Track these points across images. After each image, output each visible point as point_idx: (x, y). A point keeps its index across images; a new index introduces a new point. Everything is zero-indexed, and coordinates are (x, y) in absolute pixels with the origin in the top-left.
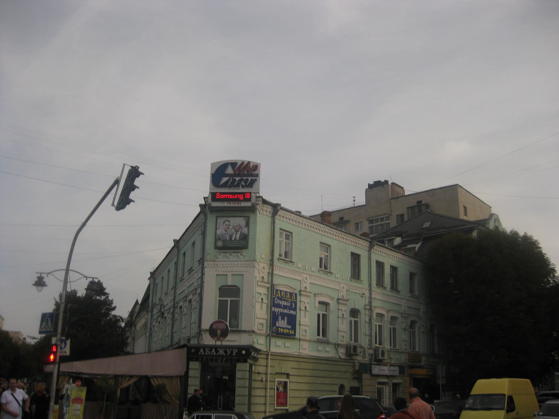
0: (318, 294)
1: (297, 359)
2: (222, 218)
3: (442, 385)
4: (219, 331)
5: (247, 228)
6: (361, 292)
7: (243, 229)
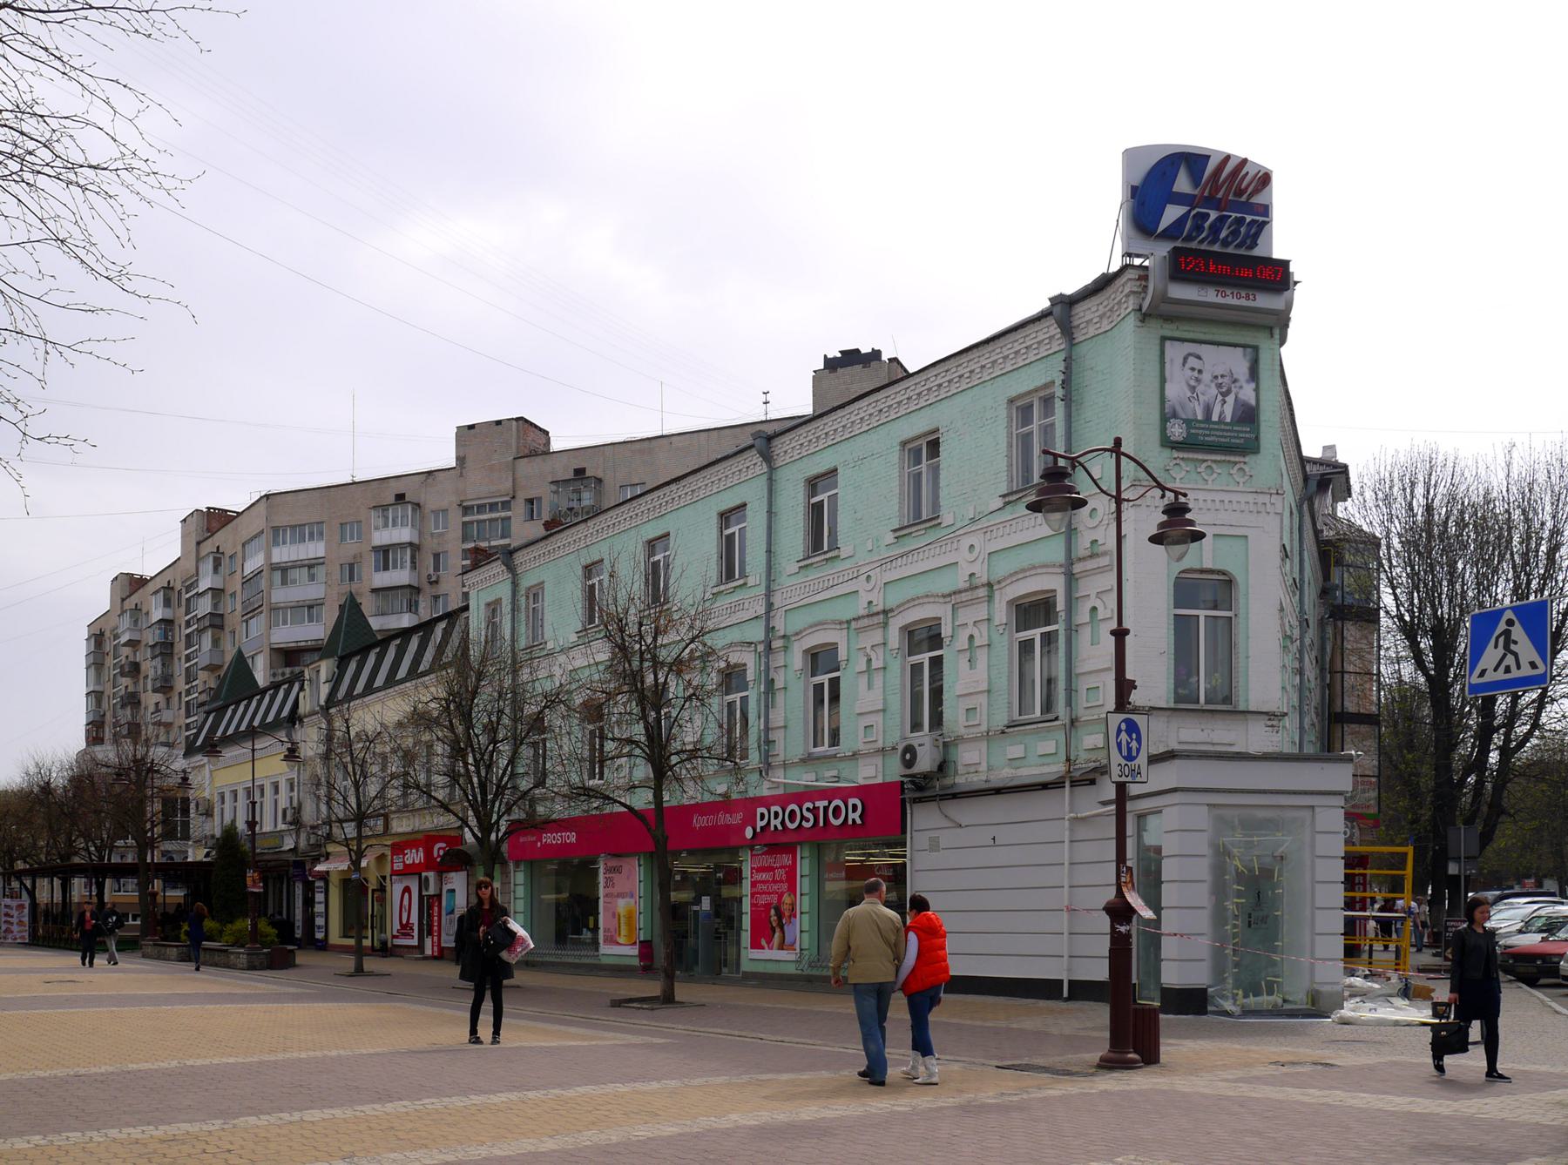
5: (1253, 385)
7: (1241, 387)
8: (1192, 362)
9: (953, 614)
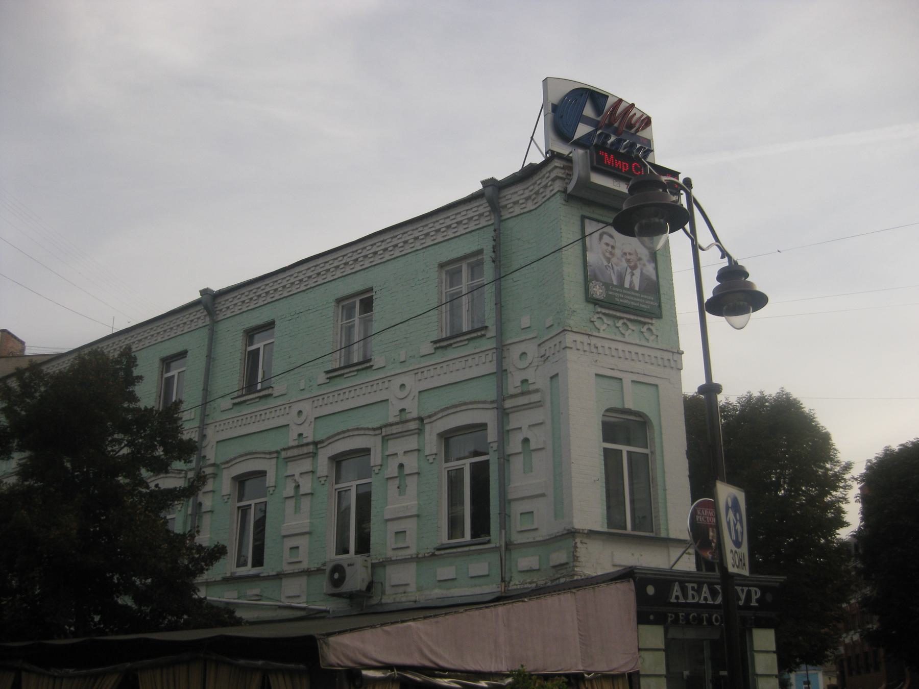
2: (594, 223)
4: (713, 532)
7: (644, 265)
8: (606, 237)
9: (382, 446)
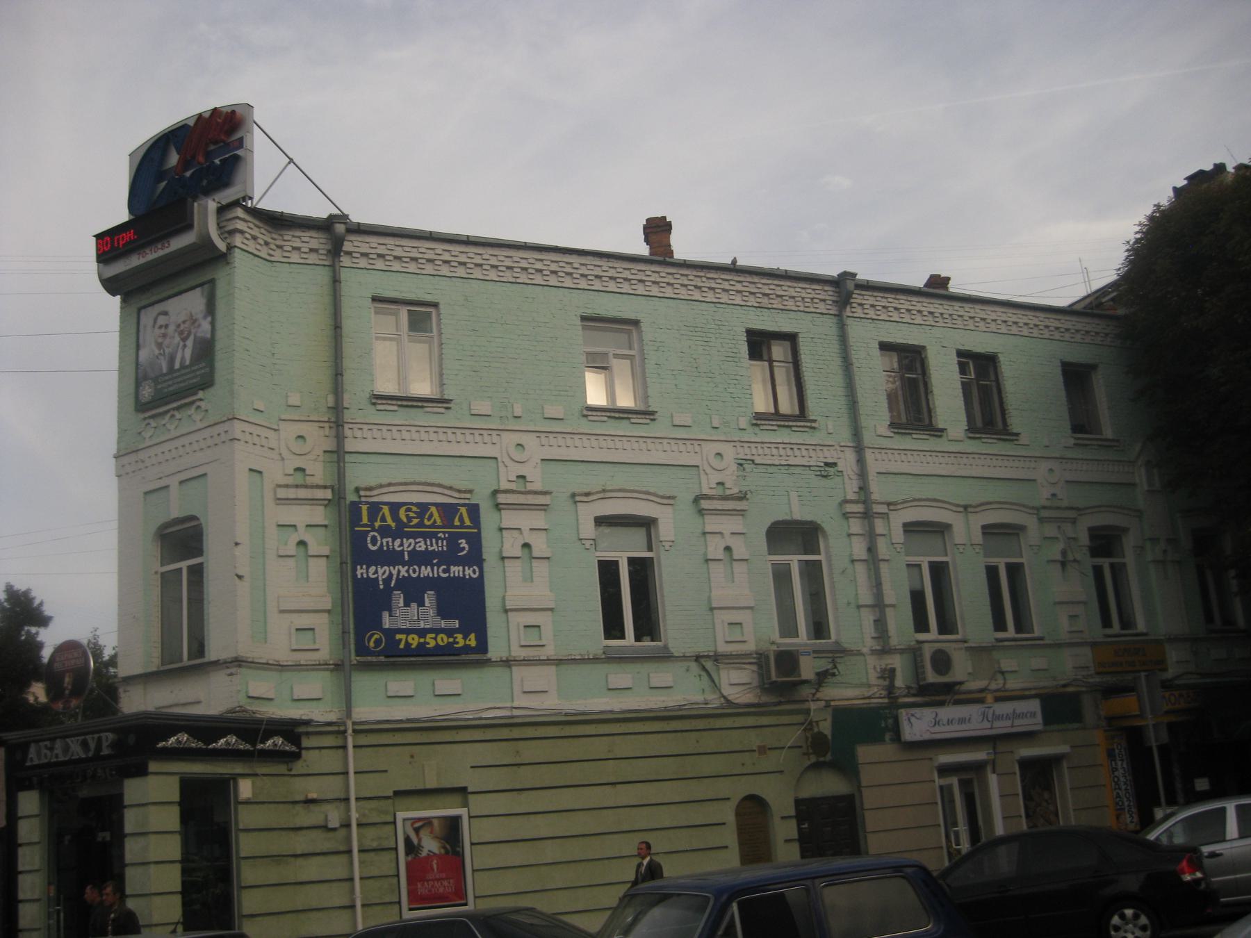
0: (587, 494)
1: (505, 733)
3: (1162, 748)
6: (818, 458)
7: (199, 326)
